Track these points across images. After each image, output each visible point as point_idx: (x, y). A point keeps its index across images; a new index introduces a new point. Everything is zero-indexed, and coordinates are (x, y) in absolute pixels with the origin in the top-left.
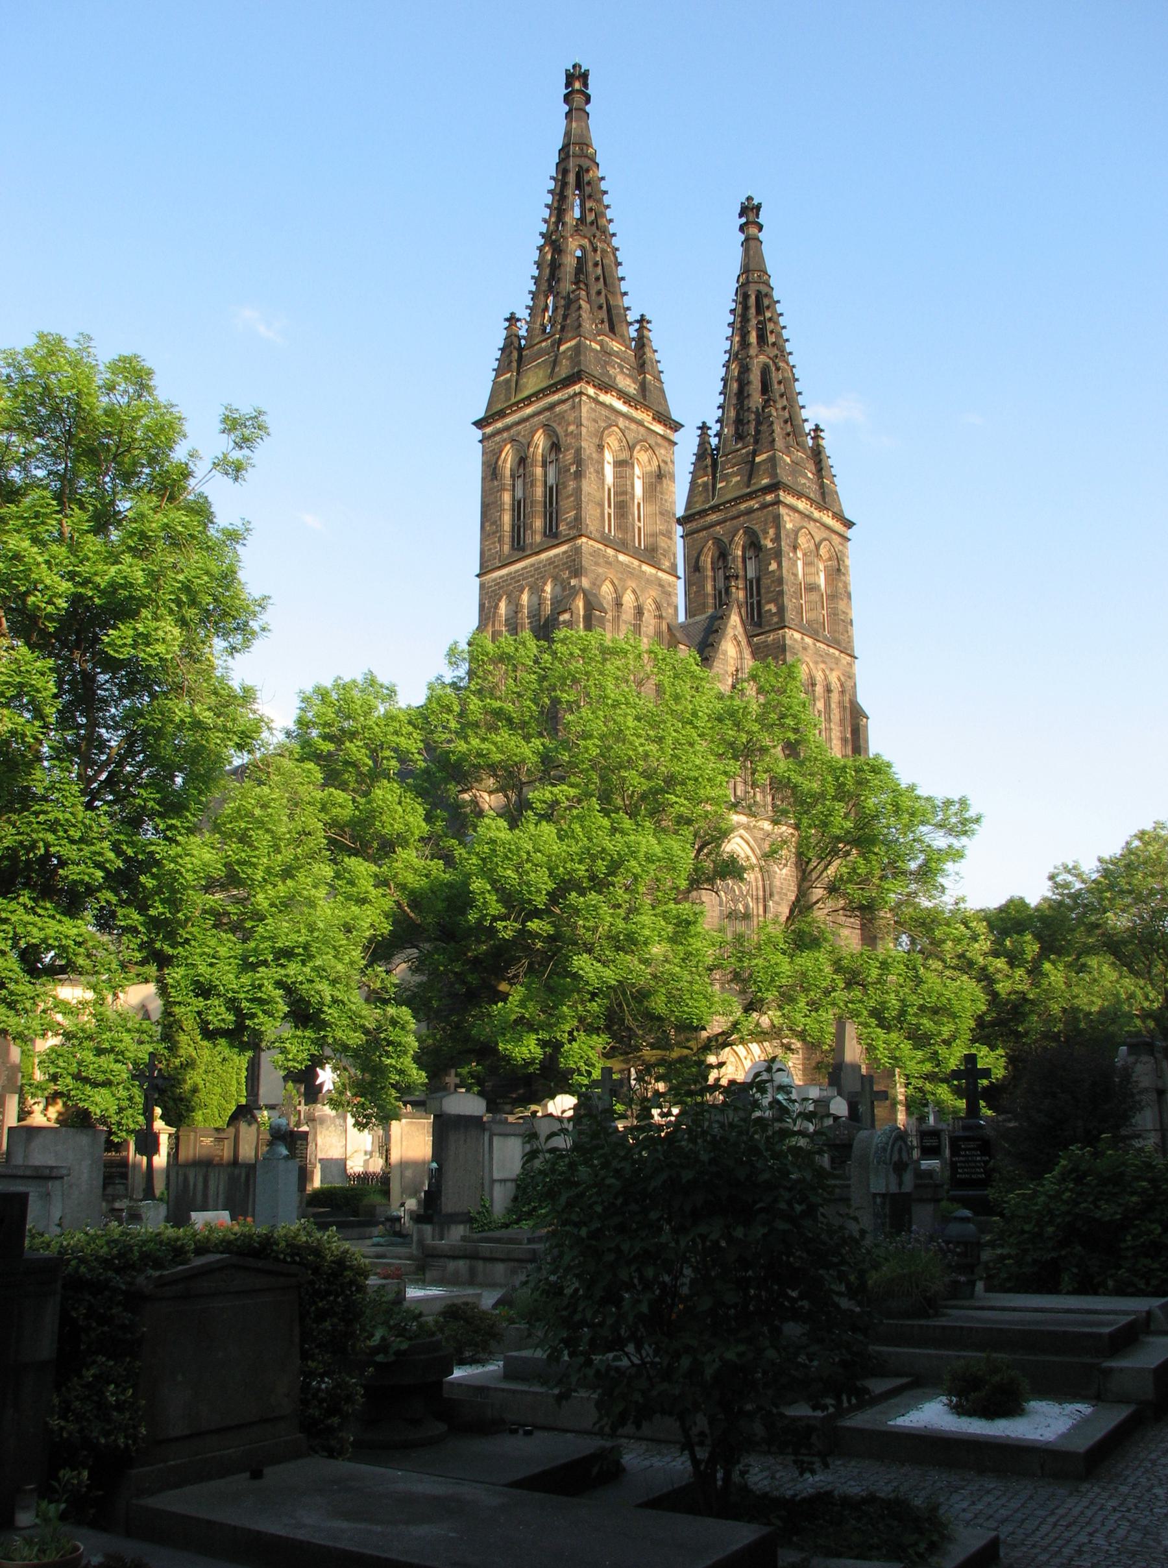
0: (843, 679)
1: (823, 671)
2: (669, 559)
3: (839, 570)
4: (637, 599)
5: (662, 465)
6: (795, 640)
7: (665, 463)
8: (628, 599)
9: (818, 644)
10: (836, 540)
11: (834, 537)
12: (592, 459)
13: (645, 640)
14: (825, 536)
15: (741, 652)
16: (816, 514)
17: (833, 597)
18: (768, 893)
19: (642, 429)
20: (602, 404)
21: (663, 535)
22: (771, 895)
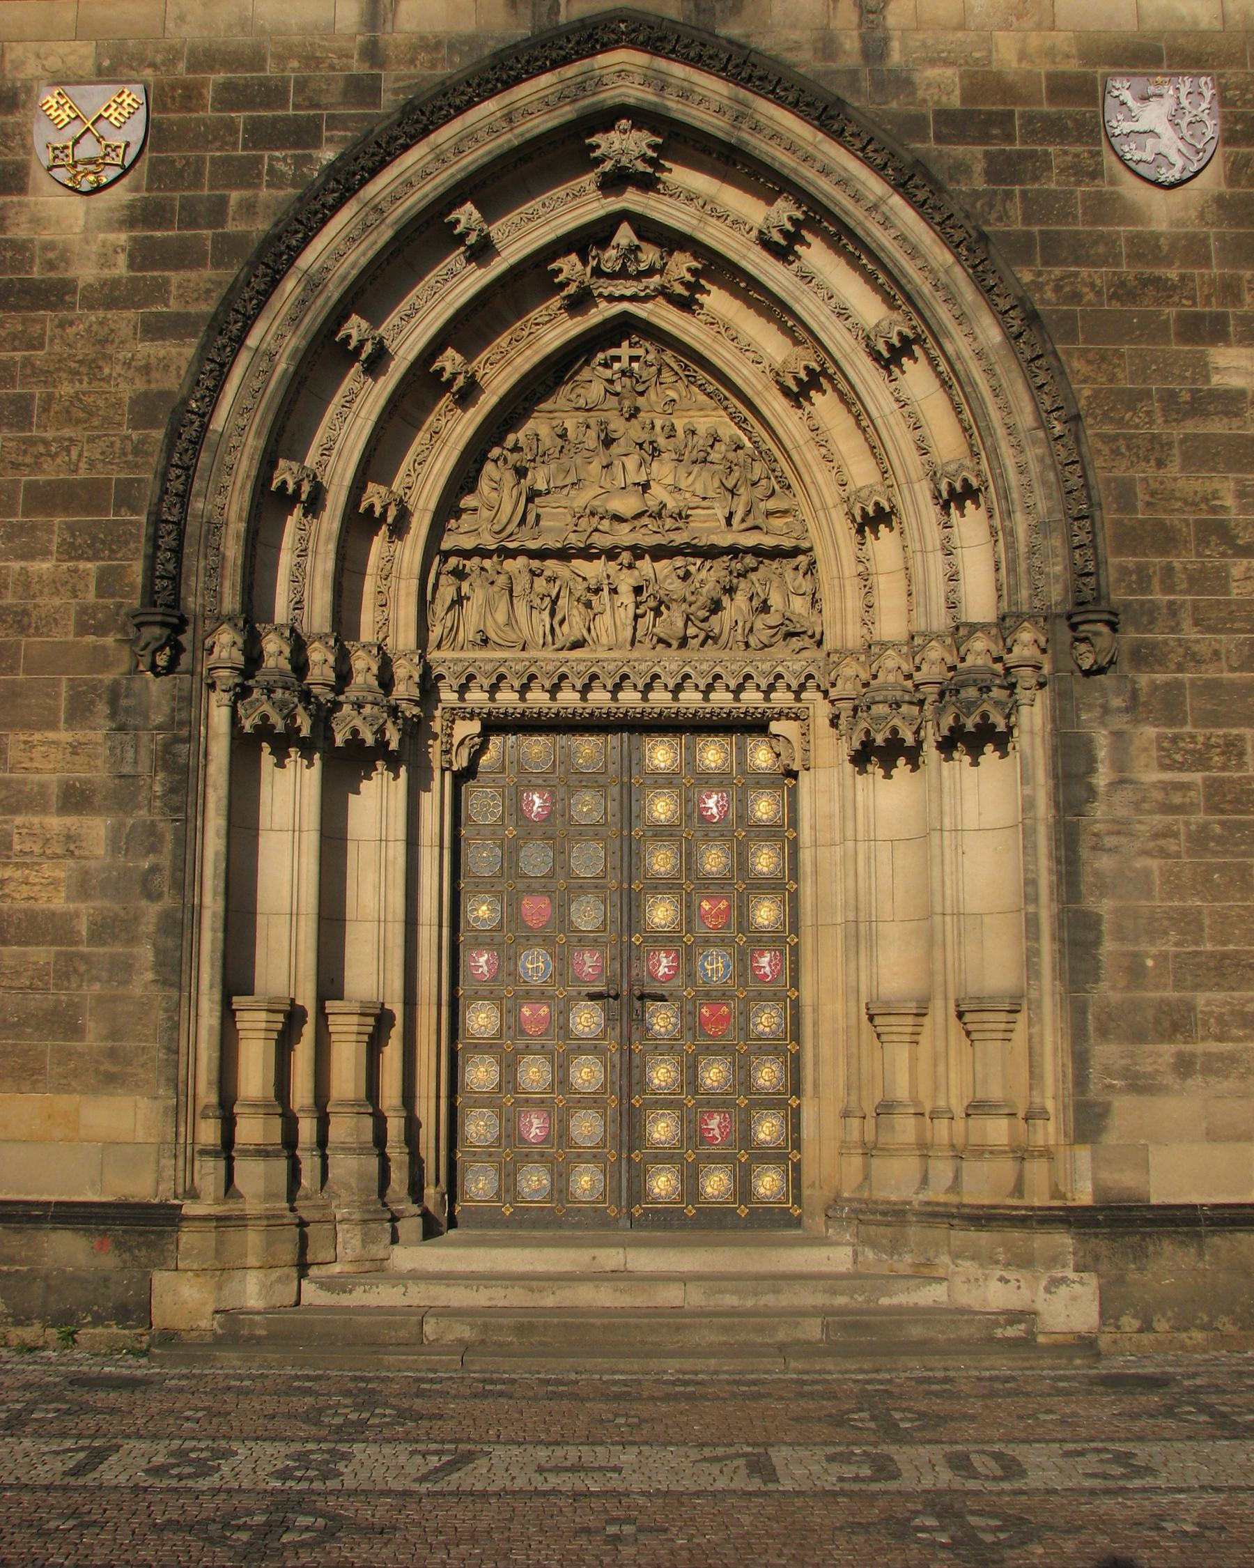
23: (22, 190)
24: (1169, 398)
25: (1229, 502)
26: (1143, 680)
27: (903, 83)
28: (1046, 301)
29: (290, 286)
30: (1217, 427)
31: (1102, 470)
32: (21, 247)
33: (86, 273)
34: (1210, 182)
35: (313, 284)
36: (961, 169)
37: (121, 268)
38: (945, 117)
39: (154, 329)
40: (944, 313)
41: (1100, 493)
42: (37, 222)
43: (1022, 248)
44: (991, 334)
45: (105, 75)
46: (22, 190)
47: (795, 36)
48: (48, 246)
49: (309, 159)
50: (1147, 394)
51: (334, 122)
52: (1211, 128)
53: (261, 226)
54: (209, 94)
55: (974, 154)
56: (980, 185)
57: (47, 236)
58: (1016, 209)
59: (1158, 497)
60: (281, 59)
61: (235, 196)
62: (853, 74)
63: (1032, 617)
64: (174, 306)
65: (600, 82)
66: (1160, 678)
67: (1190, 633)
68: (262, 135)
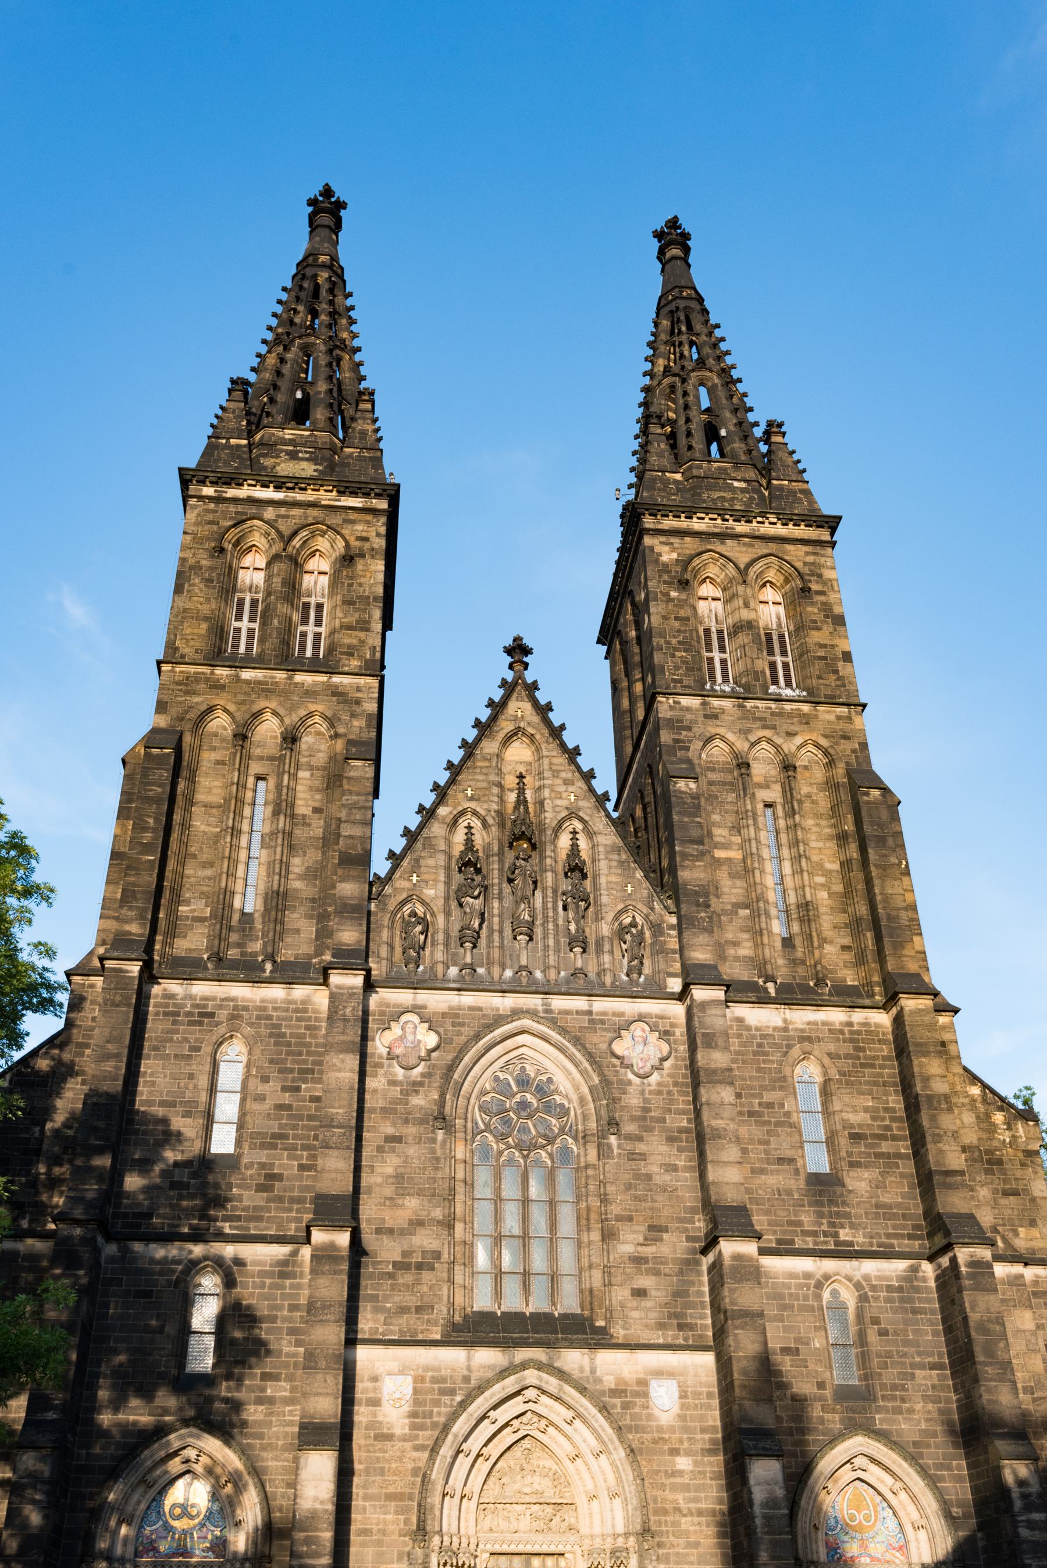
0: (824, 742)
1: (769, 741)
2: (360, 657)
3: (805, 591)
4: (282, 721)
5: (355, 544)
6: (688, 709)
7: (366, 539)
8: (269, 729)
9: (749, 704)
10: (797, 554)
11: (789, 547)
12: (201, 568)
13: (302, 774)
14: (766, 551)
15: (538, 750)
16: (741, 528)
17: (800, 629)
18: (604, 1122)
19: (314, 513)
20: (235, 500)
21: (350, 628)
22: (613, 1124)
23: (380, 1406)
24: (666, 1472)
25: (681, 1501)
26: (660, 1551)
27: (601, 1381)
28: (635, 1445)
29: (450, 1438)
30: (678, 1480)
31: (650, 1493)
32: (380, 1423)
33: (398, 1432)
34: (676, 1410)
35: (456, 1436)
36: (614, 1406)
37: (407, 1431)
38: (611, 1390)
39: (417, 1448)
40: (611, 1447)
41: (650, 1501)
42: (384, 1415)
43: (630, 1429)
44: (622, 1454)
45: (402, 1372)
46: (380, 1406)
47: (574, 1366)
48: (388, 1423)
49: (452, 1400)
50: (660, 1471)
51: (460, 1389)
52: (676, 1395)
53: (442, 1419)
54: (428, 1379)
55: (617, 1401)
56: (620, 1411)
57: (387, 1420)
58: (628, 1417)
59: (664, 1500)
60: (446, 1369)
61: (435, 1410)
62: (588, 1377)
63: (633, 1534)
64: (421, 1442)
65: (525, 1379)
66: (665, 1551)
67: (672, 1538)
68: (443, 1392)
